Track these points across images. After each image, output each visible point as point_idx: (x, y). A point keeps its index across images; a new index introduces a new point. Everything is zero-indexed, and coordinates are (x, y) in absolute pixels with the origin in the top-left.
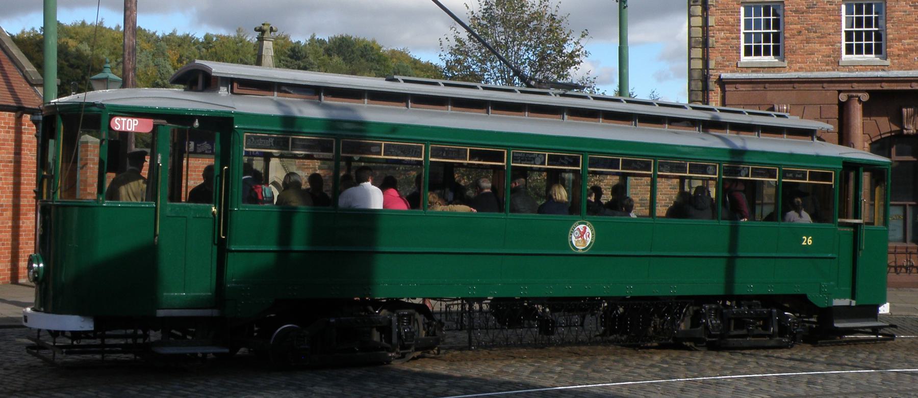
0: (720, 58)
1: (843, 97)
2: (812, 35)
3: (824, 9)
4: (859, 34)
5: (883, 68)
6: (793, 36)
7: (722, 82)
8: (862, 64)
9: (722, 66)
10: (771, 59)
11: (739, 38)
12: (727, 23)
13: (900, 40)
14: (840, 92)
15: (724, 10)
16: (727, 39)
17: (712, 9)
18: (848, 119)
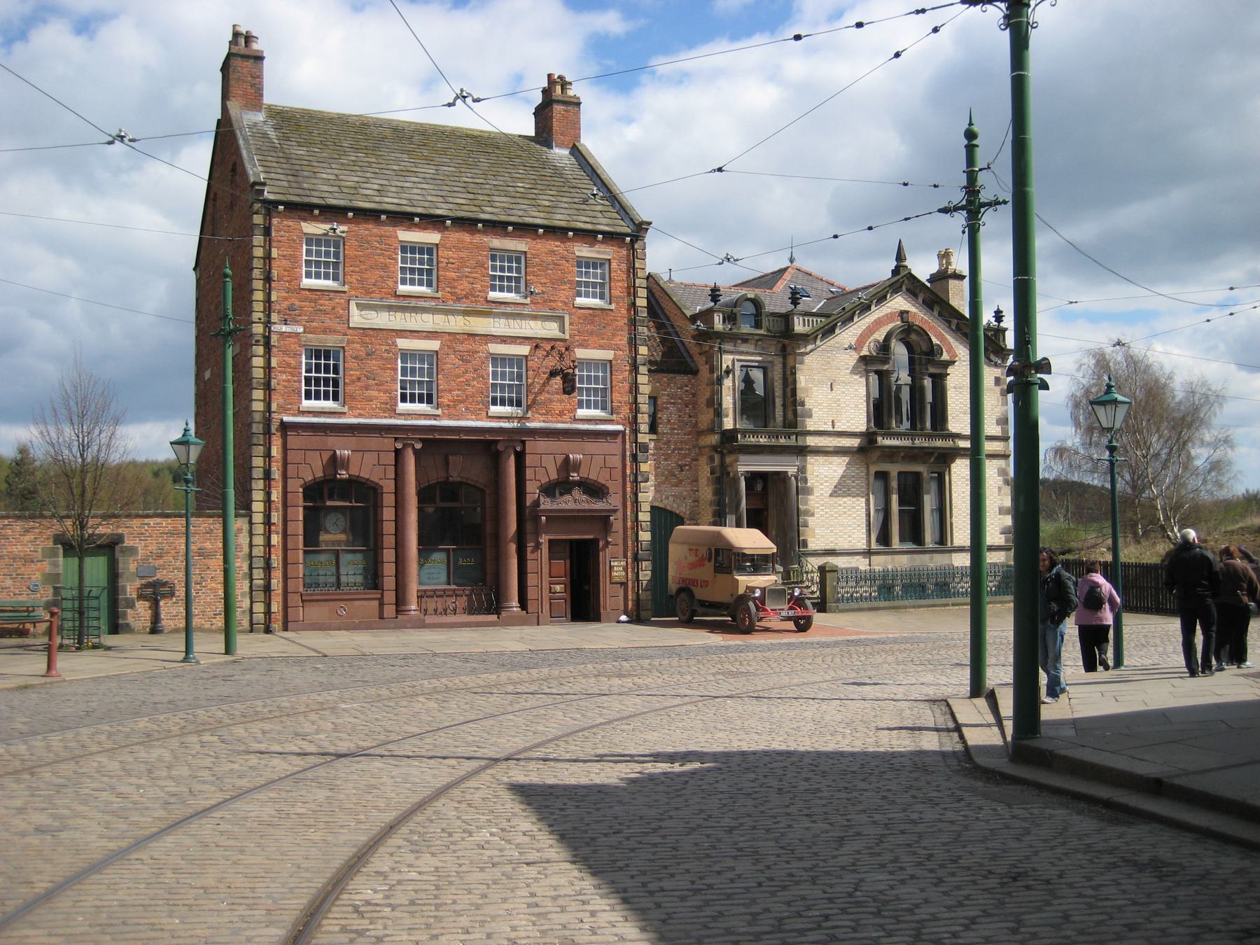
0: (281, 401)
1: (399, 446)
2: (371, 382)
3: (382, 358)
4: (317, 380)
5: (435, 417)
6: (353, 382)
7: (285, 427)
8: (414, 413)
9: (285, 410)
10: (329, 404)
11: (300, 382)
12: (289, 365)
13: (450, 391)
14: (396, 439)
15: (286, 352)
16: (289, 381)
17: (274, 350)
18: (403, 465)
